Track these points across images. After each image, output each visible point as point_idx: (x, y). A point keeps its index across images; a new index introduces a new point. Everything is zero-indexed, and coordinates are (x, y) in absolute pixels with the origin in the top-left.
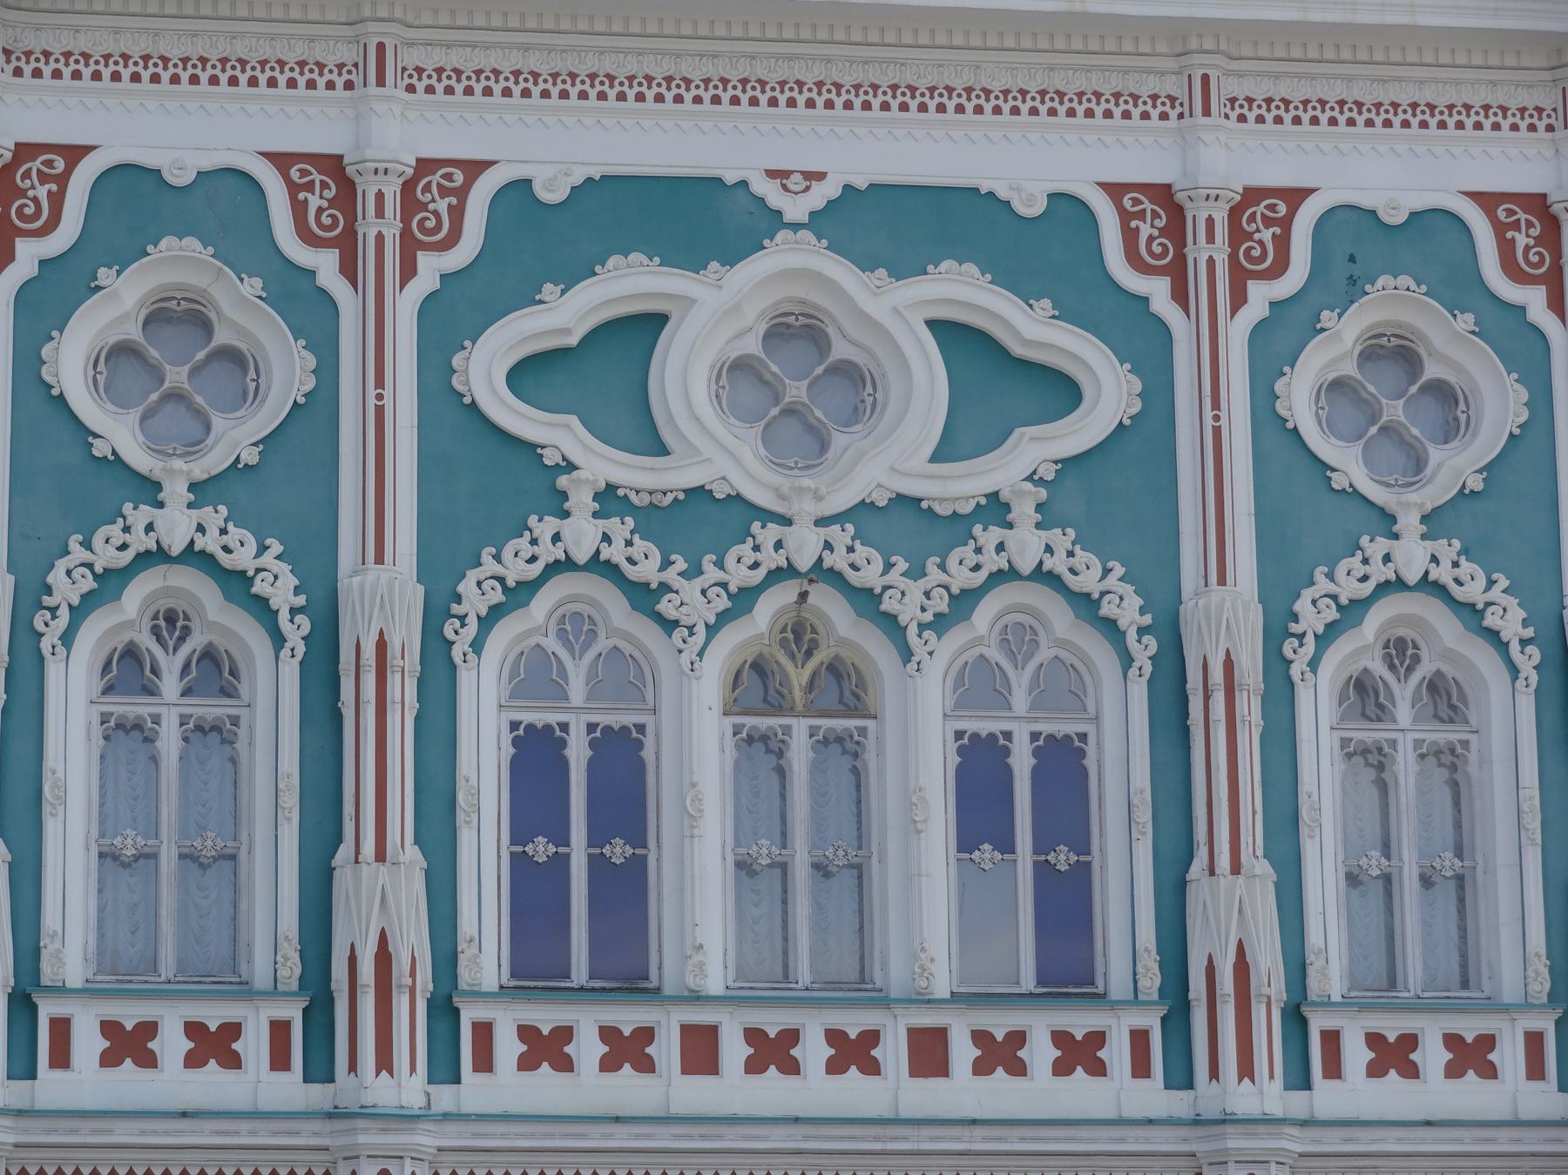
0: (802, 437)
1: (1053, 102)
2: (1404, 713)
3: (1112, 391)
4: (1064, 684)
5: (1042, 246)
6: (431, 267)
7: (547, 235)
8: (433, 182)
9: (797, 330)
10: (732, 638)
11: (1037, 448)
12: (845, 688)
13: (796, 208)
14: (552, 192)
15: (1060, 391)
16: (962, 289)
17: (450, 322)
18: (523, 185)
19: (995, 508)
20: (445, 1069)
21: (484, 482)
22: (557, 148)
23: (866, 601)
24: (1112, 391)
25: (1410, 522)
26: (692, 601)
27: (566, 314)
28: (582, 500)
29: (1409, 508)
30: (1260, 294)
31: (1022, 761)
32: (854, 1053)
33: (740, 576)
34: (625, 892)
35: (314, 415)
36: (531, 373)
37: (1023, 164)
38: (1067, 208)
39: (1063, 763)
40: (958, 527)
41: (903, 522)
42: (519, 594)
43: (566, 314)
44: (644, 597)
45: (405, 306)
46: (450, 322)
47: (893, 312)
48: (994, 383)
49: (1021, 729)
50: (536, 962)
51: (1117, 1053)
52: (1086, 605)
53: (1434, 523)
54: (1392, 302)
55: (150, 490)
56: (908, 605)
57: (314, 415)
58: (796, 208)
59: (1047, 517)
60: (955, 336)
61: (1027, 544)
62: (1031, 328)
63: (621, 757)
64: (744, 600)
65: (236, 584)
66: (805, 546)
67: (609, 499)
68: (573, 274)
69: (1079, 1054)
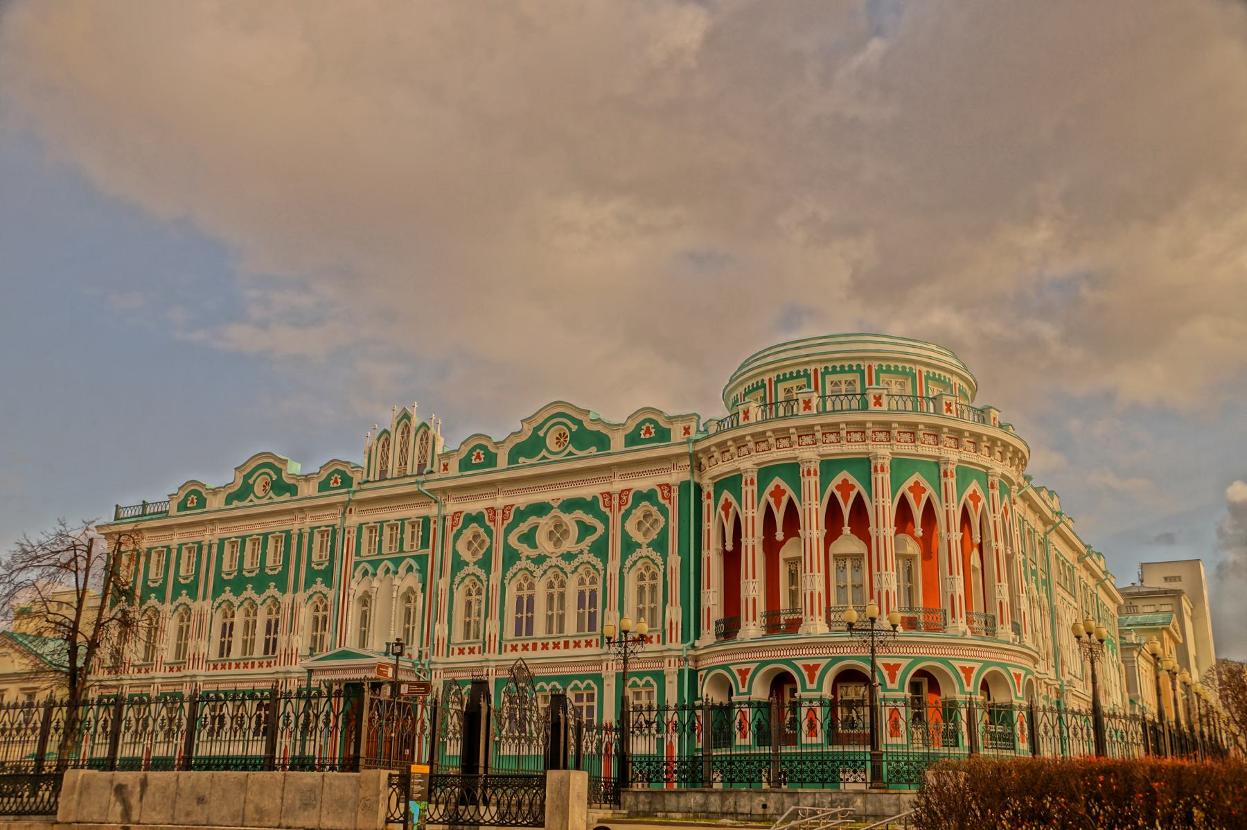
0: (557, 543)
2: (647, 578)
6: (506, 523)
7: (522, 515)
8: (507, 508)
9: (558, 526)
11: (590, 539)
12: (562, 585)
13: (555, 505)
14: (522, 508)
16: (579, 514)
17: (508, 532)
19: (581, 552)
20: (500, 653)
21: (511, 557)
22: (522, 500)
23: (562, 569)
25: (644, 546)
26: (538, 573)
27: (524, 527)
28: (524, 558)
30: (624, 509)
31: (587, 594)
34: (530, 621)
35: (490, 549)
37: (588, 491)
38: (595, 498)
39: (593, 593)
40: (576, 556)
41: (569, 557)
42: (515, 574)
43: (524, 527)
44: (531, 573)
46: (508, 532)
47: (569, 519)
48: (585, 530)
49: (587, 587)
50: (518, 632)
51: (594, 643)
53: (649, 545)
56: (568, 569)
57: (490, 549)
59: (590, 552)
60: (580, 523)
61: (586, 557)
62: (589, 519)
63: (531, 599)
64: (545, 572)
65: (478, 577)
66: (553, 561)
67: (528, 558)
69: (588, 644)
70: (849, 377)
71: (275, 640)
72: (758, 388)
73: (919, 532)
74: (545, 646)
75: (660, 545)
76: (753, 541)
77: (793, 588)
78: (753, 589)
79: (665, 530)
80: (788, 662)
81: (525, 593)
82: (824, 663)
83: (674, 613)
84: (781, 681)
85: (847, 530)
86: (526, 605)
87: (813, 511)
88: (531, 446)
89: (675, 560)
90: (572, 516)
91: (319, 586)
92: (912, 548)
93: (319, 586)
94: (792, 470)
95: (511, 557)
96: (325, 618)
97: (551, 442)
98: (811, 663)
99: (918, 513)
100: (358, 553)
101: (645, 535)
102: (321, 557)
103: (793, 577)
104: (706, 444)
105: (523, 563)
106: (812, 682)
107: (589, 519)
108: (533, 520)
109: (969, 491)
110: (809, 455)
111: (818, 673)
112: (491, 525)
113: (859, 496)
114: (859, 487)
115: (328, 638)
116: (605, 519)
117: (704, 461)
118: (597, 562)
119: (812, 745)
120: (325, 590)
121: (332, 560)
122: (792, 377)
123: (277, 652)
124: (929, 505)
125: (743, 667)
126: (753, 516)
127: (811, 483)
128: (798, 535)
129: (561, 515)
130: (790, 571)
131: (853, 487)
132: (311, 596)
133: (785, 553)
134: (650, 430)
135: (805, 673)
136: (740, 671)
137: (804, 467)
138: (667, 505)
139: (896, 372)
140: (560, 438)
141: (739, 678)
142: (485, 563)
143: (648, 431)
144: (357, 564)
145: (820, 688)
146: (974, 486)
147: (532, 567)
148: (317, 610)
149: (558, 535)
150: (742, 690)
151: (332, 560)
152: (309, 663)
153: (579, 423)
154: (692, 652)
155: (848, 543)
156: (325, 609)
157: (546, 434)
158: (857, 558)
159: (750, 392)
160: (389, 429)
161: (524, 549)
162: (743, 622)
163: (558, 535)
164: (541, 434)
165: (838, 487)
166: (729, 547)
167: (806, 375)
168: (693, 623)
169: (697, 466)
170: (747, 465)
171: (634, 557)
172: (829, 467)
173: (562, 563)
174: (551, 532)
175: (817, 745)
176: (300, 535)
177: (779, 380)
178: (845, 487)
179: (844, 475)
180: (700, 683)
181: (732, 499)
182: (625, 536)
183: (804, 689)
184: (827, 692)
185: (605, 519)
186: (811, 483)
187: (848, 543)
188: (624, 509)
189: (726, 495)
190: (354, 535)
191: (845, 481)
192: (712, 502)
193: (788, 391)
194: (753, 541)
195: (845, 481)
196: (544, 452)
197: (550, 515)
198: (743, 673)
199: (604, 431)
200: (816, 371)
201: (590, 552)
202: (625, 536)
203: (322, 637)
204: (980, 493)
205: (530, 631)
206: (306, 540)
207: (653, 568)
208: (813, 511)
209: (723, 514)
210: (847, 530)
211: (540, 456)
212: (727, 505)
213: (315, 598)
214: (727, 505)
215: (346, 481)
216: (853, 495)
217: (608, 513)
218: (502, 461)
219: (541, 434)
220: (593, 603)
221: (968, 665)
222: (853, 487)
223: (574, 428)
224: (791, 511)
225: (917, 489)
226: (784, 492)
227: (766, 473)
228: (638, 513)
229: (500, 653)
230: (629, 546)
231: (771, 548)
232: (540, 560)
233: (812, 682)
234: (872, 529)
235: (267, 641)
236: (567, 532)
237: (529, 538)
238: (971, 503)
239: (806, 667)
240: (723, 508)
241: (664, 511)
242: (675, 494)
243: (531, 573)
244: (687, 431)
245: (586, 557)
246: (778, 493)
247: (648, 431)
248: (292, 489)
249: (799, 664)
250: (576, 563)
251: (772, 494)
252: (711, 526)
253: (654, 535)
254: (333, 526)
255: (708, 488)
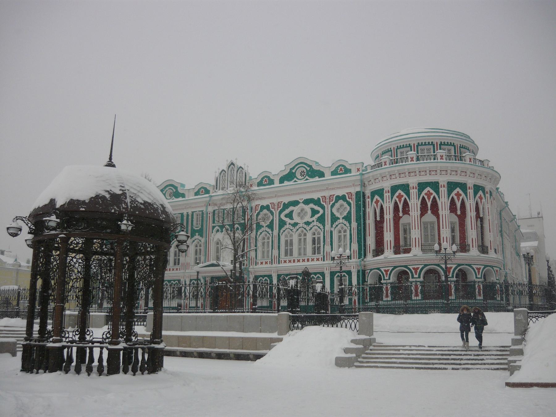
1: (317, 191)
3: (321, 211)
4: (319, 234)
5: (317, 202)
7: (286, 206)
9: (302, 210)
10: (297, 232)
11: (317, 216)
12: (305, 235)
13: (301, 202)
15: (318, 212)
16: (312, 205)
18: (284, 203)
19: (313, 221)
20: (279, 263)
21: (282, 224)
22: (286, 200)
23: (305, 229)
24: (321, 211)
25: (341, 219)
27: (287, 211)
28: (288, 224)
29: (341, 217)
32: (304, 261)
33: (297, 228)
36: (286, 216)
37: (315, 196)
38: (319, 199)
39: (319, 238)
40: (311, 223)
41: (308, 223)
43: (287, 211)
44: (291, 230)
45: (278, 212)
47: (307, 208)
48: (314, 212)
52: (319, 227)
53: (343, 218)
54: (341, 202)
55: (263, 227)
56: (308, 228)
57: (273, 220)
58: (301, 202)
59: (317, 221)
60: (312, 209)
62: (316, 208)
63: (291, 241)
64: (298, 230)
65: (268, 232)
66: (301, 225)
67: (290, 224)
68: (288, 208)
70: (428, 147)
71: (179, 260)
72: (388, 151)
73: (459, 213)
74: (299, 261)
75: (348, 218)
76: (389, 216)
77: (405, 236)
78: (388, 237)
79: (350, 213)
80: (406, 267)
81: (289, 239)
82: (421, 267)
83: (355, 246)
84: (403, 275)
85: (429, 212)
86: (289, 243)
87: (415, 203)
88: (289, 176)
89: (354, 224)
90: (309, 206)
91: (197, 236)
92: (456, 219)
93: (197, 236)
94: (405, 188)
95: (282, 224)
96: (200, 250)
97: (298, 175)
98: (416, 267)
99: (458, 205)
100: (214, 222)
101: (341, 214)
102: (197, 224)
103: (405, 231)
104: (366, 176)
105: (287, 226)
106: (416, 274)
107: (316, 208)
108: (291, 208)
109: (478, 195)
110: (413, 181)
111: (418, 271)
112: (273, 210)
113: (434, 198)
114: (434, 194)
115: (203, 258)
116: (323, 207)
117: (366, 183)
118: (319, 225)
119: (415, 300)
120: (200, 238)
121: (202, 226)
122: (403, 147)
123: (180, 264)
124: (463, 200)
125: (386, 269)
126: (389, 206)
127: (414, 192)
128: (409, 214)
129: (304, 205)
130: (404, 229)
131: (432, 194)
132: (194, 241)
133: (402, 221)
134: (341, 169)
135: (413, 271)
136: (385, 271)
137: (411, 186)
138: (351, 201)
139: (448, 144)
140: (302, 174)
141: (384, 273)
142: (271, 226)
143: (341, 170)
144: (214, 227)
145: (419, 277)
146: (480, 193)
147: (292, 228)
148: (196, 246)
149: (302, 213)
150: (386, 278)
151: (202, 226)
152: (197, 268)
153: (310, 166)
154: (363, 263)
155: (429, 217)
156: (200, 246)
157: (296, 171)
158: (432, 223)
159: (385, 153)
160: (225, 169)
161: (287, 220)
162: (386, 250)
163: (302, 213)
164: (294, 171)
165: (426, 194)
166: (378, 219)
167: (410, 146)
168: (362, 252)
169: (363, 185)
170: (387, 185)
171: (337, 223)
172: (422, 186)
173: (305, 226)
174: (299, 213)
175: (419, 300)
176: (188, 215)
177: (398, 148)
178: (429, 194)
179: (428, 189)
180: (366, 275)
181: (379, 199)
182: (332, 214)
183: (413, 277)
184: (421, 279)
185: (323, 207)
186: (414, 192)
187: (429, 217)
188: (331, 203)
189: (377, 197)
190: (211, 215)
191: (429, 191)
192: (370, 200)
193: (402, 153)
194: (389, 216)
195: (429, 191)
196: (295, 179)
197: (299, 206)
198: (386, 271)
199: (322, 170)
200: (414, 144)
201: (317, 221)
202: (332, 214)
203: (200, 258)
204: (483, 196)
205: (291, 255)
206: (190, 217)
207: (345, 227)
208: (415, 203)
209: (375, 205)
210: (429, 212)
211: (294, 180)
212: (377, 202)
213: (196, 241)
214: (377, 202)
215: (207, 192)
216: (432, 197)
217: (325, 205)
218: (277, 184)
219: (294, 171)
220: (319, 243)
221: (479, 267)
222: (432, 194)
223: (308, 169)
224: (406, 204)
225: (458, 195)
226: (402, 196)
227: (394, 189)
228: (337, 205)
229: (279, 263)
230: (334, 219)
231: (397, 219)
232: (295, 225)
233: (416, 274)
234: (440, 212)
235: (175, 260)
236: (306, 212)
237: (290, 215)
238: (479, 200)
239: (414, 268)
240: (375, 203)
241: (349, 204)
242: (354, 197)
243: (291, 230)
244: (358, 170)
245: (315, 223)
246: (400, 197)
247: (341, 170)
248: (183, 196)
249: (411, 267)
250: (311, 226)
251: (397, 197)
252: (370, 211)
253: (345, 214)
254: (202, 211)
255: (368, 193)
